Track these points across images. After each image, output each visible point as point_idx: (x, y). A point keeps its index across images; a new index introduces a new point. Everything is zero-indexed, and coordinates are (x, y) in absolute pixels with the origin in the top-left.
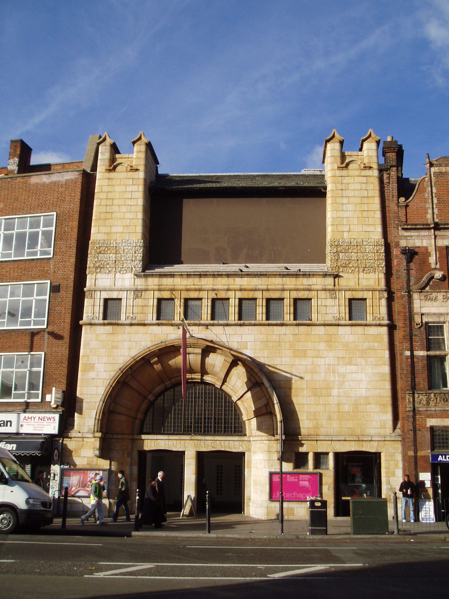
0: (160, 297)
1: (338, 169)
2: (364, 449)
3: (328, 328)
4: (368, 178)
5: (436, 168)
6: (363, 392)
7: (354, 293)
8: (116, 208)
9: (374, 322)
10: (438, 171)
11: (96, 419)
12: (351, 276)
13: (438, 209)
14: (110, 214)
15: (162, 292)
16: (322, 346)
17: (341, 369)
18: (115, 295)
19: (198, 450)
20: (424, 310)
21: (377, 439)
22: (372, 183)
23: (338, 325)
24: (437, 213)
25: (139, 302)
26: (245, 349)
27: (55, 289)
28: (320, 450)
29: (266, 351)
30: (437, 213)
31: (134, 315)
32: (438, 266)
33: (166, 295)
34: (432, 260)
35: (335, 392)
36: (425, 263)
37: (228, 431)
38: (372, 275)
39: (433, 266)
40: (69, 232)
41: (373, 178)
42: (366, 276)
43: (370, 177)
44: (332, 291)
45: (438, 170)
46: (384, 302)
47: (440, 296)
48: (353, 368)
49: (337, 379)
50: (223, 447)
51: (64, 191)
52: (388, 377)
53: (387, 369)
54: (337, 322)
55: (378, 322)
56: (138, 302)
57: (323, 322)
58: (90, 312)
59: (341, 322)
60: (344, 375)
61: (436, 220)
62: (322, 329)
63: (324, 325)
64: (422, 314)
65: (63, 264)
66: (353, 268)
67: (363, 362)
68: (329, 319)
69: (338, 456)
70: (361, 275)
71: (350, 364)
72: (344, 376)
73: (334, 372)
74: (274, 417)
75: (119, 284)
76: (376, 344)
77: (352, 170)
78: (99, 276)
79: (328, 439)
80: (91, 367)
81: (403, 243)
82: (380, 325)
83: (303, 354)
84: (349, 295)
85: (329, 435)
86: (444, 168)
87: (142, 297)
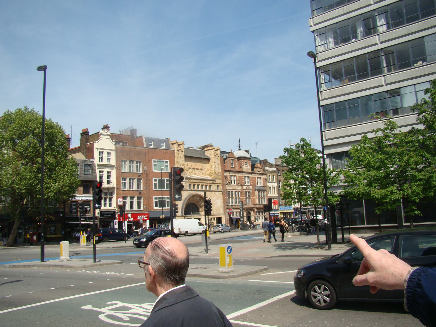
16: (214, 196)
20: (228, 189)
28: (214, 217)
33: (190, 183)
35: (216, 205)
36: (227, 179)
48: (218, 200)
69: (217, 218)
71: (217, 199)
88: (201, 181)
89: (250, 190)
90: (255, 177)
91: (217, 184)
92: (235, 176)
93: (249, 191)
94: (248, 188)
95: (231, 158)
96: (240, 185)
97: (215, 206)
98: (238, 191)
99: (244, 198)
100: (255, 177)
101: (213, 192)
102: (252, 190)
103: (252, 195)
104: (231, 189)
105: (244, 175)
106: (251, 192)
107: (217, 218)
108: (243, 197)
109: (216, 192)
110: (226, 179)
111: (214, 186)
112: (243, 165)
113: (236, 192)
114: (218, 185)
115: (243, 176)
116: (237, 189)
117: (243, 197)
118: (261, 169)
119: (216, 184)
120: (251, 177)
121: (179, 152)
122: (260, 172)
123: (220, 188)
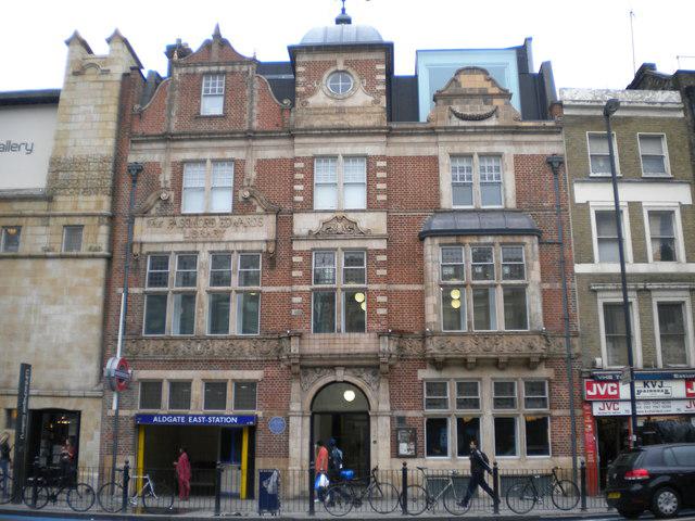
3: (34, 261)
6: (68, 338)
7: (69, 219)
12: (69, 199)
16: (26, 282)
17: (47, 310)
20: (145, 238)
23: (46, 257)
32: (169, 185)
35: (34, 337)
38: (93, 198)
39: (163, 186)
42: (86, 198)
44: (45, 218)
46: (104, 229)
47: (166, 220)
48: (57, 308)
52: (99, 320)
53: (97, 310)
55: (91, 253)
57: (28, 254)
62: (28, 264)
63: (31, 257)
64: (142, 244)
67: (70, 302)
68: (38, 251)
70: (81, 198)
71: (54, 302)
72: (46, 317)
76: (87, 280)
77: (89, 75)
81: (132, 159)
82: (93, 257)
84: (64, 221)
89: (365, 235)
90: (435, 159)
91: (64, 215)
93: (355, 244)
94: (340, 226)
96: (267, 212)
97: (28, 340)
98: (240, 247)
99: (292, 294)
100: (435, 159)
102: (379, 238)
103: (382, 272)
104: (180, 237)
106: (379, 252)
108: (288, 289)
109: (50, 264)
110: (140, 186)
111: (42, 230)
112: (311, 92)
113: (220, 259)
114: (77, 221)
115: (296, 159)
117: (288, 289)
120: (383, 158)
122: (492, 122)
123: (100, 238)
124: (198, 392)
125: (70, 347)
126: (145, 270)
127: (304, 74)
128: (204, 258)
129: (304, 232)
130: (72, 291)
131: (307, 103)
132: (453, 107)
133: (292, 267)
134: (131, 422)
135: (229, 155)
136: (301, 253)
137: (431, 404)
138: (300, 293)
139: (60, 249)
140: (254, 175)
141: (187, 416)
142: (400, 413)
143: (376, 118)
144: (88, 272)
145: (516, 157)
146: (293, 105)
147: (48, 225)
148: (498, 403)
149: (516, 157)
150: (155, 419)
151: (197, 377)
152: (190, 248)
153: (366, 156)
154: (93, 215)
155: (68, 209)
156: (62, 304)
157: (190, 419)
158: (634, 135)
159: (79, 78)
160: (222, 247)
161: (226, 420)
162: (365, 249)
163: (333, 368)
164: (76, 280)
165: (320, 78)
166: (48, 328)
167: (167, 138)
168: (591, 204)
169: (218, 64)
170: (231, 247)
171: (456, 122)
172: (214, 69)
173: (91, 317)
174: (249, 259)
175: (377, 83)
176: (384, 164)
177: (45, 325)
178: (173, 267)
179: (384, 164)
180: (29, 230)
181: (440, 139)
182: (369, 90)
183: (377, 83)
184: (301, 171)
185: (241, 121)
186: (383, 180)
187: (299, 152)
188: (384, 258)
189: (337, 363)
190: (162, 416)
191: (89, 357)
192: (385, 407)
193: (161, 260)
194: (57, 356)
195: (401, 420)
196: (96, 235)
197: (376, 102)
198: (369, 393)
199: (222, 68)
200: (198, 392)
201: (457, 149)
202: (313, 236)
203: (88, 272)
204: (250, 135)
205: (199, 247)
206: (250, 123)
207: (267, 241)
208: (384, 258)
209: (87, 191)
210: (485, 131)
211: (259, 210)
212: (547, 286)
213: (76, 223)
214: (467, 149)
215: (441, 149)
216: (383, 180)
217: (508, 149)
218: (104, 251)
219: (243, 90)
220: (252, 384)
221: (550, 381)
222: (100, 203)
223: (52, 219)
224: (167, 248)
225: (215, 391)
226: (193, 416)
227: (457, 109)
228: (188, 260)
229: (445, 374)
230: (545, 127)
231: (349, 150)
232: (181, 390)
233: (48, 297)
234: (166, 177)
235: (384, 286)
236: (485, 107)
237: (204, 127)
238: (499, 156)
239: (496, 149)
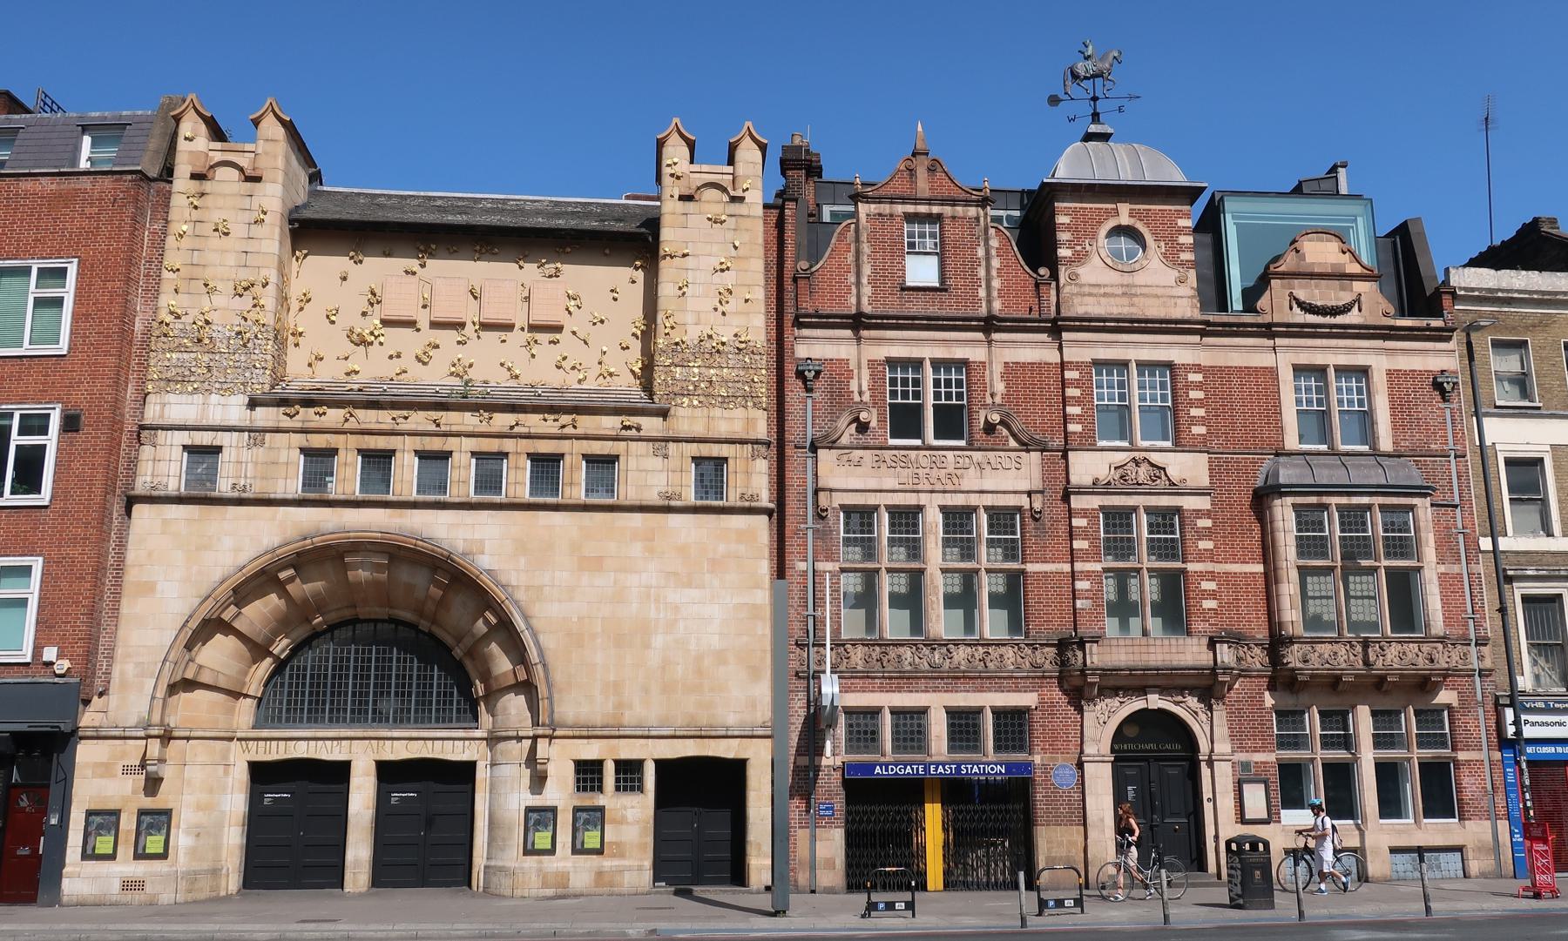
0: (305, 444)
1: (679, 200)
2: (711, 754)
4: (740, 220)
5: (873, 206)
6: (715, 642)
7: (702, 446)
8: (210, 257)
9: (739, 504)
10: (876, 211)
11: (153, 698)
13: (873, 287)
14: (201, 269)
15: (309, 435)
16: (636, 549)
17: (674, 596)
18: (205, 439)
19: (379, 758)
20: (832, 484)
21: (736, 733)
22: (747, 230)
23: (668, 510)
24: (870, 295)
25: (259, 452)
26: (480, 554)
27: (71, 424)
28: (624, 756)
29: (522, 560)
30: (870, 295)
31: (248, 481)
32: (866, 397)
34: (854, 386)
35: (658, 641)
37: (423, 718)
38: (739, 413)
40: (106, 303)
41: (748, 219)
42: (726, 413)
43: (742, 218)
45: (875, 209)
47: (868, 455)
48: (694, 593)
49: (662, 616)
50: (430, 750)
51: (95, 214)
54: (666, 503)
55: (747, 504)
56: (257, 455)
58: (149, 473)
59: (673, 503)
60: (676, 607)
61: (867, 309)
65: (92, 371)
66: (702, 398)
68: (653, 498)
69: (660, 764)
70: (717, 412)
71: (689, 585)
72: (676, 608)
73: (657, 601)
74: (534, 691)
75: (216, 418)
76: (742, 548)
77: (708, 202)
78: (171, 398)
79: (640, 733)
80: (149, 588)
81: (802, 351)
83: (595, 564)
85: (644, 725)
86: (888, 206)
87: (266, 445)
88: (469, 421)
89: (1175, 489)
90: (1272, 373)
92: (963, 364)
93: (1165, 501)
94: (1143, 473)
95: (900, 209)
98: (989, 500)
100: (1272, 373)
101: (638, 518)
104: (890, 483)
105: (1082, 349)
106: (1199, 513)
107: (660, 764)
111: (657, 462)
112: (1080, 258)
113: (957, 519)
116: (971, 480)
118: (1359, 286)
119: (677, 440)
120: (1198, 368)
121: (207, 186)
122: (1353, 318)
124: (938, 727)
125: (720, 657)
126: (839, 534)
127: (1068, 228)
128: (933, 520)
129: (1088, 481)
130: (716, 565)
131: (1077, 276)
132: (1295, 292)
133: (1071, 534)
134: (838, 775)
135: (959, 353)
136: (1084, 513)
137: (1283, 743)
138: (1088, 575)
139: (690, 497)
140: (1000, 387)
141: (927, 767)
142: (1242, 757)
143: (1185, 306)
144: (741, 536)
145: (1389, 373)
146: (1055, 276)
147: (666, 456)
148: (1379, 742)
149: (1389, 373)
150: (878, 770)
151: (937, 704)
152: (910, 500)
153: (1170, 365)
154: (743, 442)
155: (699, 430)
156: (701, 586)
157: (932, 768)
158: (1560, 341)
159: (690, 206)
160: (959, 500)
161: (988, 769)
162: (1178, 510)
163: (1142, 691)
164: (722, 548)
165: (1094, 236)
166: (681, 624)
167: (857, 323)
168: (1498, 447)
169: (929, 201)
170: (974, 500)
171: (1300, 317)
172: (923, 209)
173: (755, 606)
174: (1001, 518)
175: (1182, 248)
176: (1198, 377)
177: (676, 620)
178: (883, 527)
179: (1198, 377)
180: (632, 463)
181: (1279, 341)
182: (1171, 258)
183: (1182, 248)
184: (1076, 384)
185: (975, 300)
186: (1200, 403)
187: (1071, 354)
188: (1207, 523)
189: (1151, 682)
190: (886, 766)
191: (754, 673)
192: (1223, 747)
193: (861, 516)
194: (699, 672)
195: (1245, 766)
196: (748, 473)
197: (1181, 281)
198: (1196, 728)
199: (936, 209)
200: (938, 727)
201: (1304, 359)
202: (1096, 488)
203: (741, 536)
204: (990, 325)
205: (923, 499)
206: (989, 302)
207: (1029, 494)
208: (1207, 523)
209: (725, 402)
210: (1346, 332)
211: (1013, 443)
212: (1442, 569)
213: (715, 454)
214: (1318, 359)
215: (1284, 357)
216: (1200, 403)
217: (1380, 360)
218: (765, 500)
219: (973, 248)
220: (1020, 713)
221: (1449, 707)
222: (749, 422)
223: (671, 445)
224: (871, 500)
225: (963, 725)
226: (937, 765)
227: (1301, 295)
228: (906, 518)
229: (1304, 698)
230: (1429, 328)
231: (1147, 354)
232: (911, 724)
233: (676, 574)
234: (860, 384)
235: (1209, 566)
236: (1342, 294)
237: (917, 307)
238: (1364, 372)
239: (1360, 360)
